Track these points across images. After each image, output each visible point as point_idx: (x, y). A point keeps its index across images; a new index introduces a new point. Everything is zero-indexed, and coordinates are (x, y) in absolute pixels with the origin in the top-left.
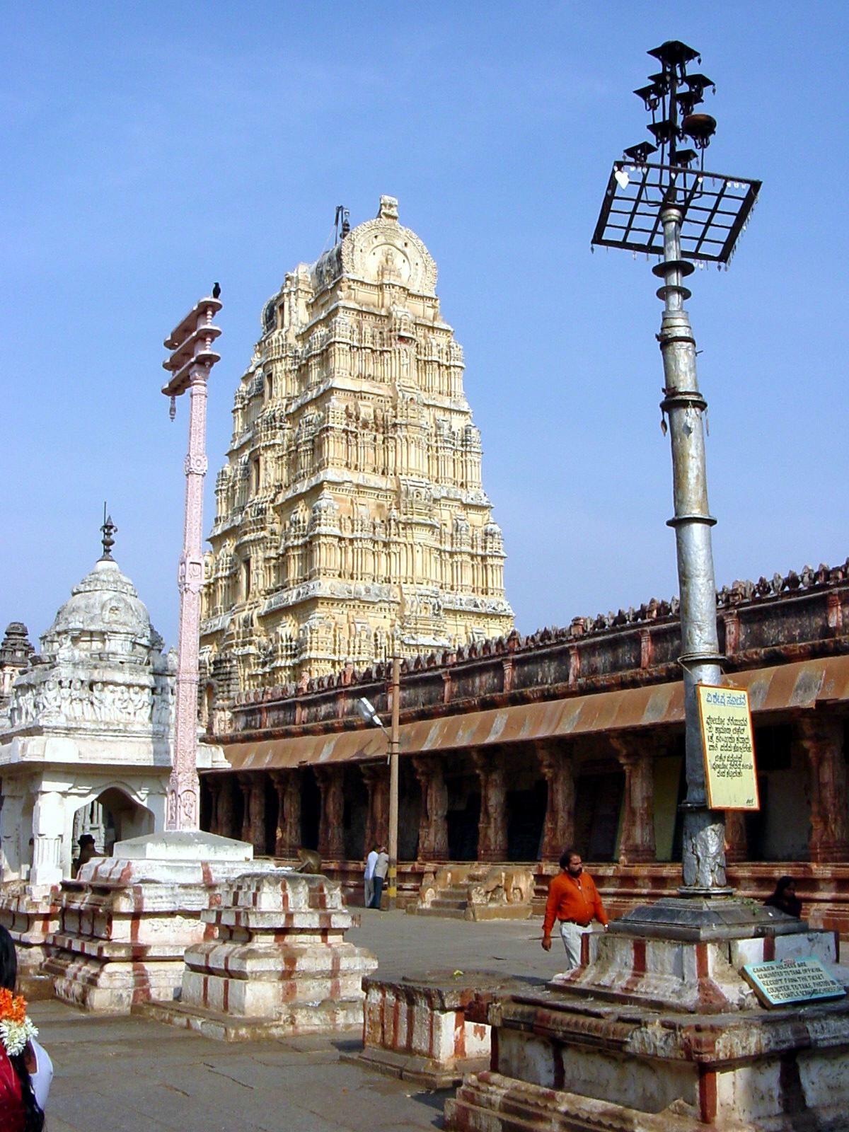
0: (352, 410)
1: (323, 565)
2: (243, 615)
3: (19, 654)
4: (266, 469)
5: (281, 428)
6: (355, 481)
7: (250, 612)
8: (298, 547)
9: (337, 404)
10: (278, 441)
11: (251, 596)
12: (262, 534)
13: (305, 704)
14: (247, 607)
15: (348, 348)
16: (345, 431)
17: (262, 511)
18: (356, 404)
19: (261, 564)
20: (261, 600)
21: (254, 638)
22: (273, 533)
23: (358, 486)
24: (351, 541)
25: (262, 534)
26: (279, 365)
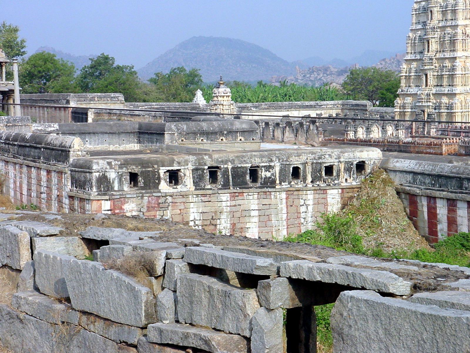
0: (464, 32)
1: (457, 83)
2: (426, 92)
3: (402, 127)
4: (432, 45)
5: (437, 31)
6: (466, 55)
7: (429, 92)
8: (447, 75)
9: (459, 30)
10: (436, 36)
11: (428, 86)
12: (432, 67)
13: (463, 132)
14: (427, 90)
15: (462, 10)
16: (462, 40)
17: (431, 59)
18: (465, 29)
19: (431, 76)
20: (433, 88)
21: (431, 100)
22: (436, 67)
23: (466, 56)
24: (465, 74)
25: (432, 67)
26: (435, 8)
